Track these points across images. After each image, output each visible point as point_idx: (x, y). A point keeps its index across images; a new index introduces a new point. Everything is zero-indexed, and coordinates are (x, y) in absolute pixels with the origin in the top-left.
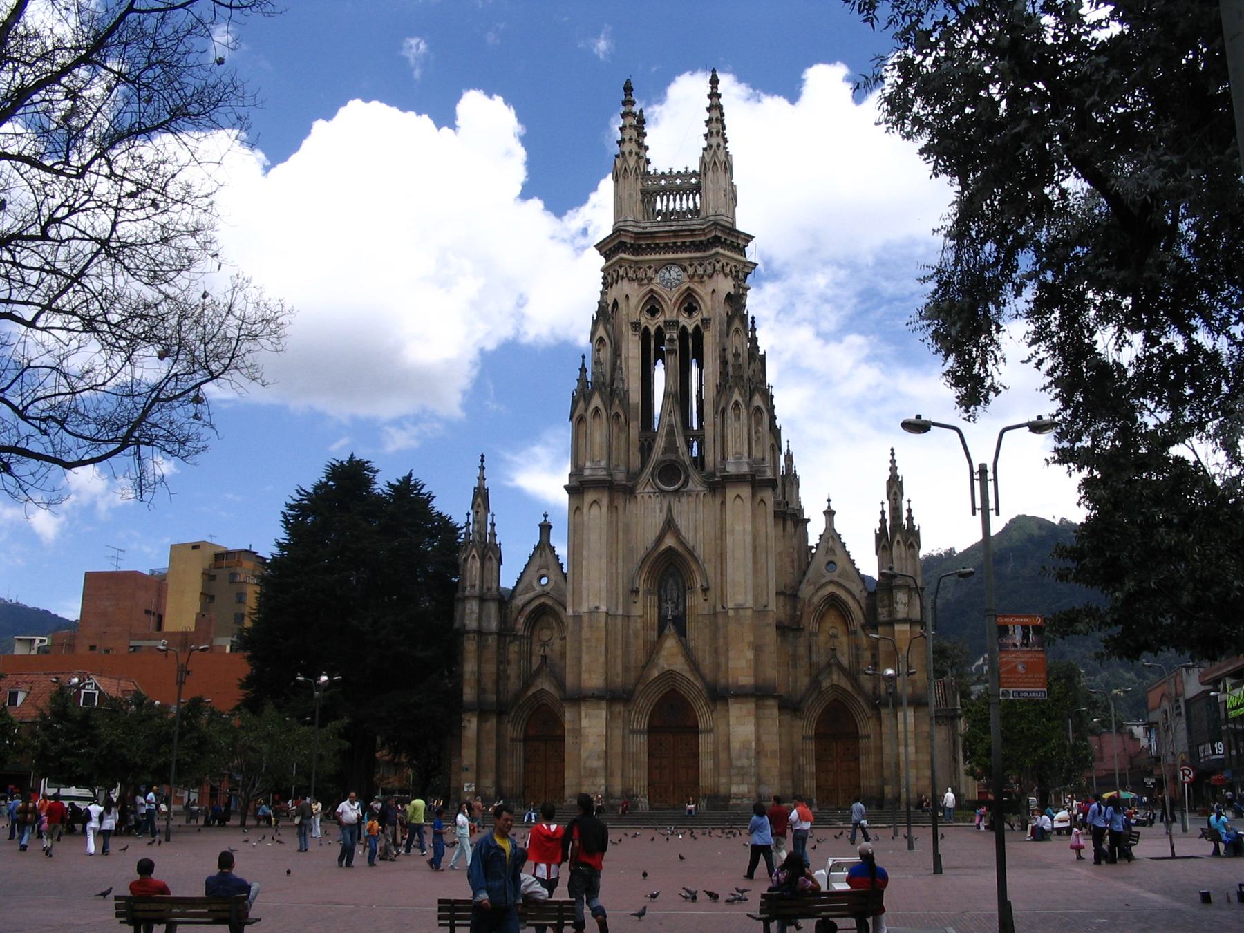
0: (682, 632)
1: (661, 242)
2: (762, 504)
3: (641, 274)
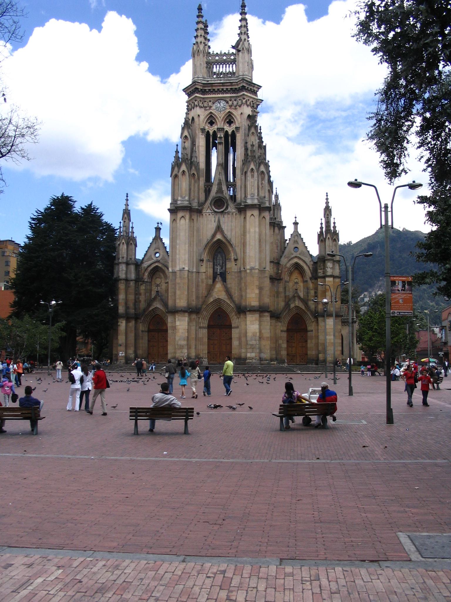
0: (224, 280)
1: (216, 88)
2: (264, 219)
3: (206, 105)
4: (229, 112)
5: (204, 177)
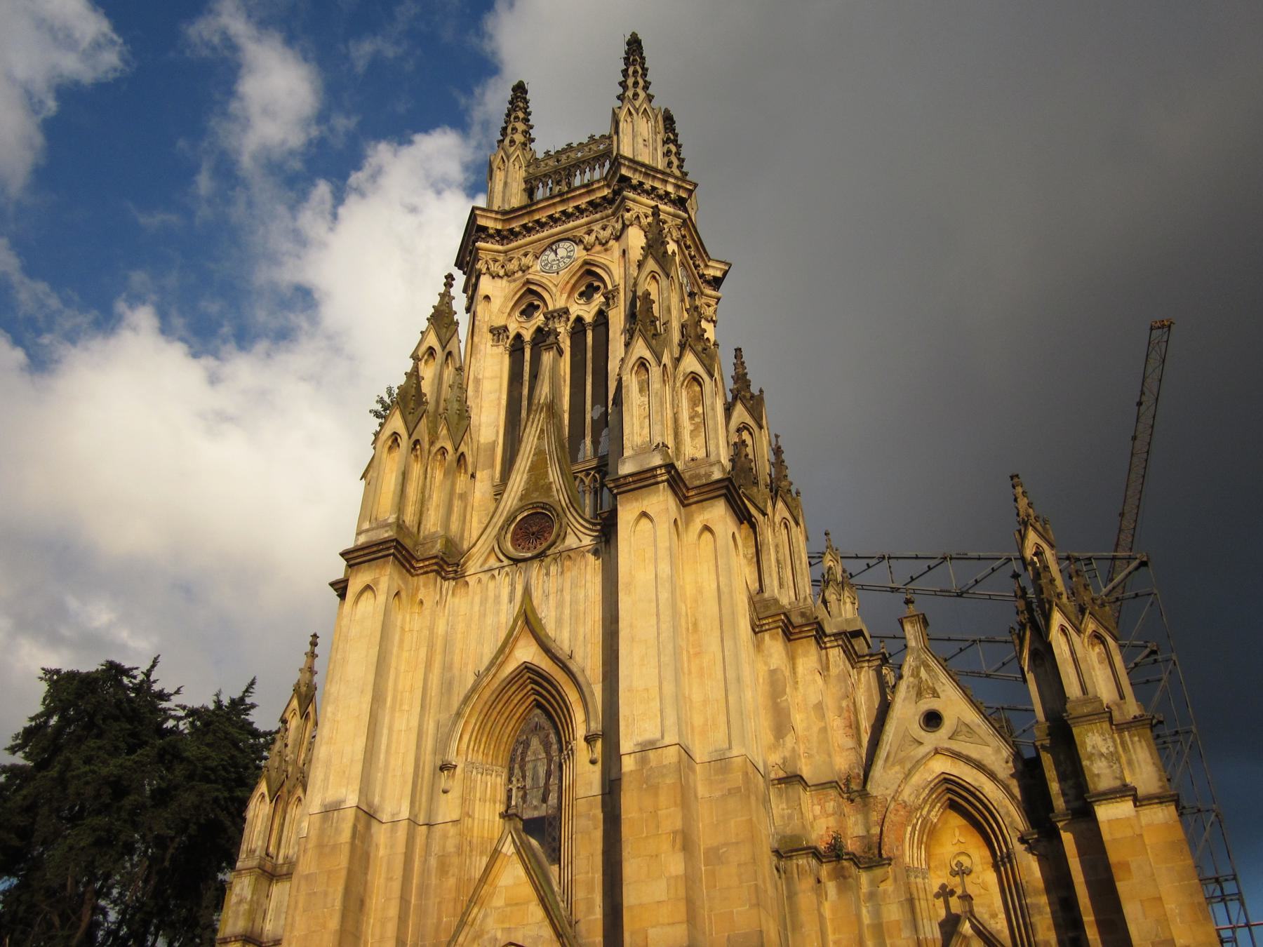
2: (707, 535)
3: (513, 266)
4: (586, 263)
5: (492, 466)
